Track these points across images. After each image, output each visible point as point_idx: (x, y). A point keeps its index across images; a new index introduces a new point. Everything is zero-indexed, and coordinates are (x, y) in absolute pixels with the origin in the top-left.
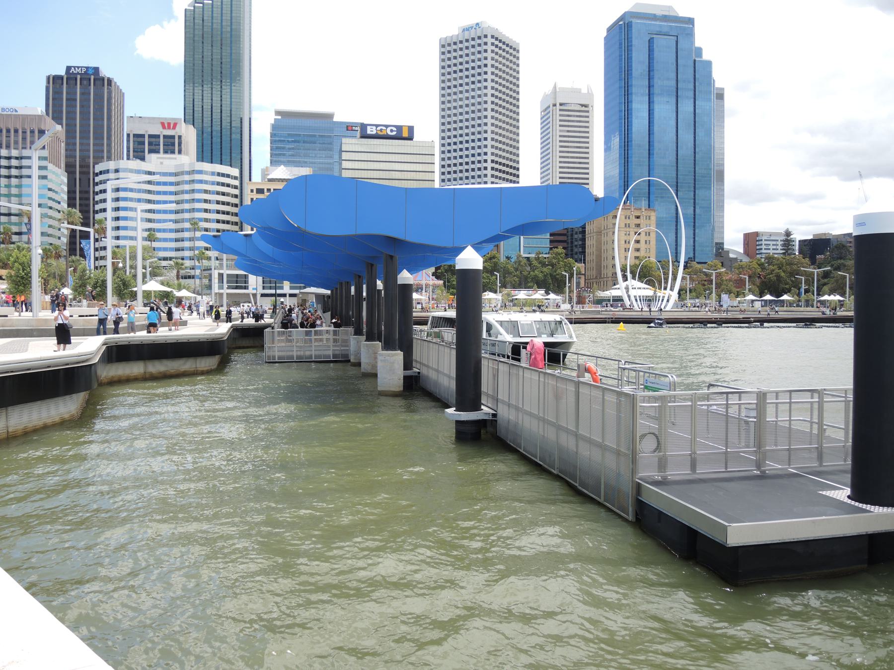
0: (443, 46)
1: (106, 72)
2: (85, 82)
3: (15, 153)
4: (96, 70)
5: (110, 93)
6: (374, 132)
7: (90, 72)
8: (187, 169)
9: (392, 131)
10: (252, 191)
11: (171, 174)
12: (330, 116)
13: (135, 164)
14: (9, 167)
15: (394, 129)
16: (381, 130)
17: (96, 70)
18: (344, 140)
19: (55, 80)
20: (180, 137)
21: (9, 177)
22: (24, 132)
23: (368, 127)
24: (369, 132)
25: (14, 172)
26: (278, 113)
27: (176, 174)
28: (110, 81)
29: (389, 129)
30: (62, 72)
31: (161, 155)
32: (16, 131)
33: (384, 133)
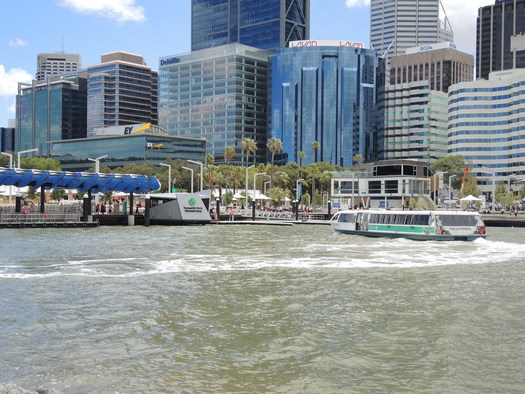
3: (406, 85)
11: (505, 88)
13: (482, 83)
14: (401, 98)
19: (485, 10)
21: (401, 105)
22: (433, 65)
25: (405, 101)
31: (503, 72)
32: (427, 65)
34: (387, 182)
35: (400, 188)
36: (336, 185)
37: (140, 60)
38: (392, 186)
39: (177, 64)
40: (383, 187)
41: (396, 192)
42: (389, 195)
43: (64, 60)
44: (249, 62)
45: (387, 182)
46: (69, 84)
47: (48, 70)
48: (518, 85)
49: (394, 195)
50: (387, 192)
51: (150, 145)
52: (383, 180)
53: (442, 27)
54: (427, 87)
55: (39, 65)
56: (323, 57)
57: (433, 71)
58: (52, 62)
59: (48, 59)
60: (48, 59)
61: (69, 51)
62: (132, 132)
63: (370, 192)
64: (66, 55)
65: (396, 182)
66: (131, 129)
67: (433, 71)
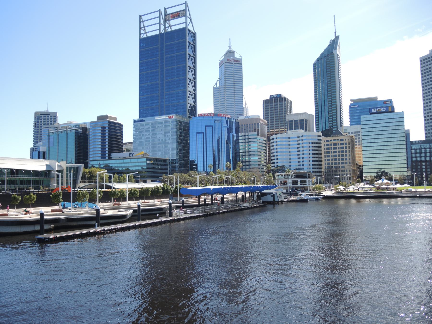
0: (421, 61)
1: (284, 95)
2: (276, 101)
3: (247, 134)
4: (280, 95)
5: (285, 104)
6: (376, 111)
7: (278, 96)
8: (301, 135)
9: (383, 109)
10: (324, 141)
12: (374, 99)
13: (284, 135)
15: (385, 108)
16: (379, 110)
17: (280, 95)
18: (361, 116)
20: (306, 120)
23: (373, 110)
24: (373, 111)
26: (351, 100)
27: (298, 137)
28: (285, 99)
29: (382, 109)
30: (268, 98)
31: (294, 130)
33: (380, 111)
34: (301, 181)
35: (307, 183)
36: (278, 181)
37: (116, 119)
38: (303, 183)
40: (299, 183)
41: (306, 185)
42: (302, 186)
44: (180, 122)
45: (301, 181)
46: (77, 130)
48: (302, 136)
49: (304, 186)
50: (301, 185)
51: (148, 162)
52: (299, 180)
53: (244, 106)
54: (255, 135)
55: (35, 118)
57: (252, 126)
58: (43, 116)
61: (51, 110)
63: (292, 185)
64: (50, 112)
65: (306, 181)
66: (133, 154)
67: (252, 126)
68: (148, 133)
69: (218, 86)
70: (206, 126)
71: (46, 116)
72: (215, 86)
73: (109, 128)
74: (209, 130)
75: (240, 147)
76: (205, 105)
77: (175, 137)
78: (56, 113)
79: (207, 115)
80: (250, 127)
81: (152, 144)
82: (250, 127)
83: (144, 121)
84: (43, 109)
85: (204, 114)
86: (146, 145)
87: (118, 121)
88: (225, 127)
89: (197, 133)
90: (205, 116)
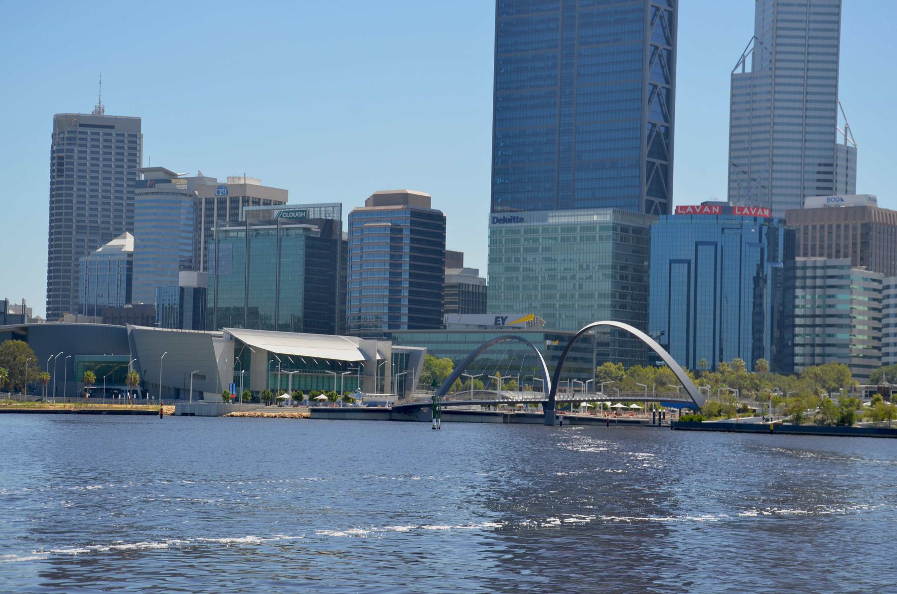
39: (520, 224)
43: (113, 127)
44: (625, 229)
47: (80, 145)
51: (548, 342)
53: (840, 140)
56: (723, 229)
58: (89, 130)
59: (81, 125)
60: (81, 125)
62: (506, 322)
64: (116, 119)
66: (504, 320)
68: (530, 258)
69: (748, 69)
70: (697, 244)
71: (101, 131)
72: (739, 71)
73: (412, 231)
74: (706, 253)
75: (798, 302)
76: (700, 174)
77: (609, 272)
78: (136, 122)
79: (701, 212)
80: (838, 236)
81: (544, 287)
82: (838, 236)
83: (521, 220)
84: (85, 108)
85: (693, 207)
86: (525, 287)
87: (434, 206)
88: (751, 245)
89: (671, 262)
90: (695, 212)
